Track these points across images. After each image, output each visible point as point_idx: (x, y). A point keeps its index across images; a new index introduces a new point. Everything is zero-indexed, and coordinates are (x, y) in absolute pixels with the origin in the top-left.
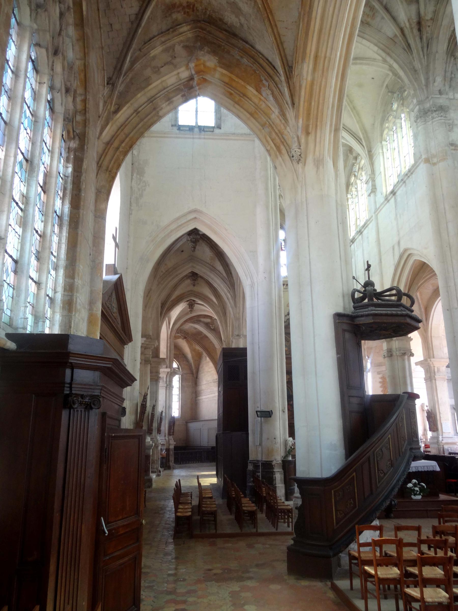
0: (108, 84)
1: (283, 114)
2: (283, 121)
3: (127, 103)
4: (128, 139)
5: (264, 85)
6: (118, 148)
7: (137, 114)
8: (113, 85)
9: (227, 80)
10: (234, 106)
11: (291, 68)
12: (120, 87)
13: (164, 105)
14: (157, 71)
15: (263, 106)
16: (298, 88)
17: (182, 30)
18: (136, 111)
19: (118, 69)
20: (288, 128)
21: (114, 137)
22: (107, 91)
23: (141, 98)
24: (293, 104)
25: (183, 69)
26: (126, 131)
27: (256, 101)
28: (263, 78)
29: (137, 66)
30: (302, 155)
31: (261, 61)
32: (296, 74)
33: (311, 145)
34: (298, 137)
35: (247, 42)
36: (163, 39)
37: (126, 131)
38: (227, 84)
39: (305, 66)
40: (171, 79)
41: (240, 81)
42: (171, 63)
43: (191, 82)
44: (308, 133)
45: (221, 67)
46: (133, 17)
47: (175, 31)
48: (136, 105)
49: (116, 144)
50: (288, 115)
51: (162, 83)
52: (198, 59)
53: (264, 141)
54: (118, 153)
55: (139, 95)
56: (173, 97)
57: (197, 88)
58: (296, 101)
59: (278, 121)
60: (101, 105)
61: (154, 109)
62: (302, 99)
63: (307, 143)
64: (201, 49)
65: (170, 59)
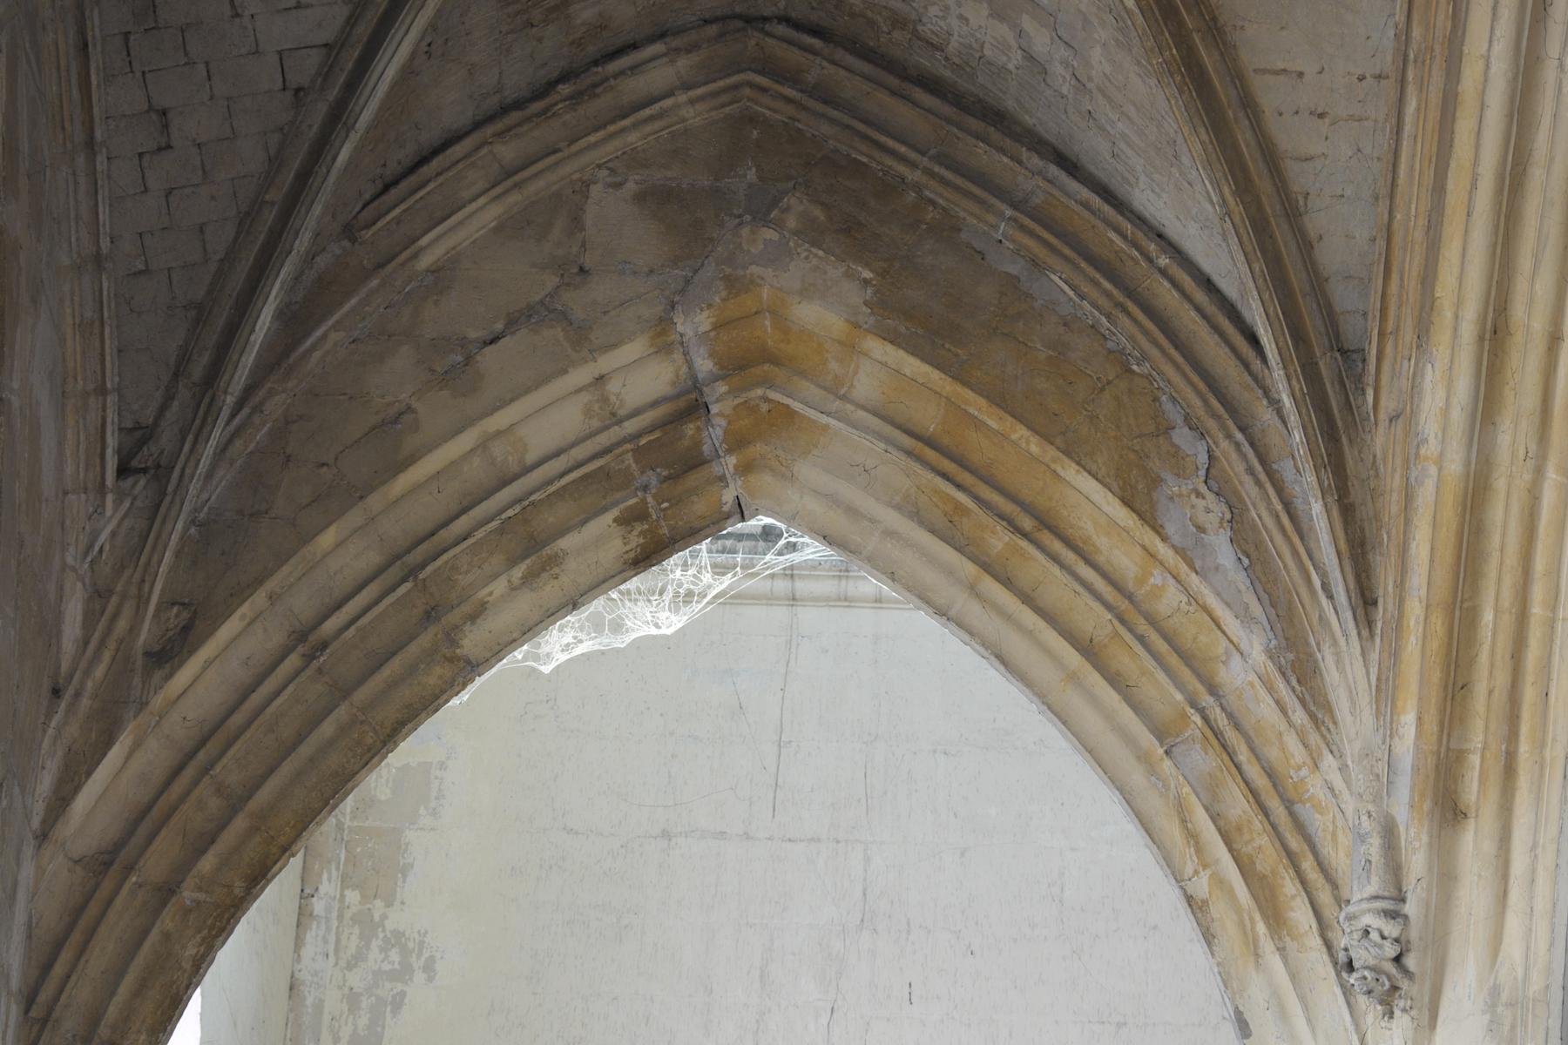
0: (123, 471)
1: (1299, 668)
2: (1299, 716)
3: (241, 593)
4: (240, 823)
5: (1176, 457)
6: (167, 891)
7: (310, 658)
8: (160, 472)
9: (929, 418)
10: (973, 589)
11: (1349, 356)
12: (204, 486)
13: (499, 587)
14: (457, 369)
15: (1170, 600)
16: (1393, 504)
17: (636, 86)
18: (306, 640)
19: (197, 376)
20: (1329, 761)
21: (143, 820)
22: (113, 518)
23: (342, 550)
24: (1365, 600)
25: (634, 349)
26: (231, 771)
27: (1125, 562)
28: (1173, 414)
29: (328, 339)
30: (1410, 962)
31: (1167, 297)
32: (1388, 404)
33: (1473, 895)
34: (1389, 833)
35: (1072, 167)
36: (507, 152)
37: (231, 771)
38: (929, 442)
39: (1432, 378)
40: (547, 419)
41: (1020, 433)
42: (559, 320)
43: (690, 429)
44: (1448, 809)
45: (894, 339)
46: (306, 67)
47: (591, 92)
48: (303, 604)
49: (156, 862)
50: (1331, 675)
51: (483, 445)
52: (735, 285)
53: (1172, 831)
54: (167, 920)
55: (327, 538)
56: (563, 532)
57: (732, 461)
58: (1385, 584)
59: (1264, 710)
60: (74, 611)
61: (431, 615)
62: (1418, 580)
63: (1445, 876)
64: (762, 210)
65: (552, 281)
